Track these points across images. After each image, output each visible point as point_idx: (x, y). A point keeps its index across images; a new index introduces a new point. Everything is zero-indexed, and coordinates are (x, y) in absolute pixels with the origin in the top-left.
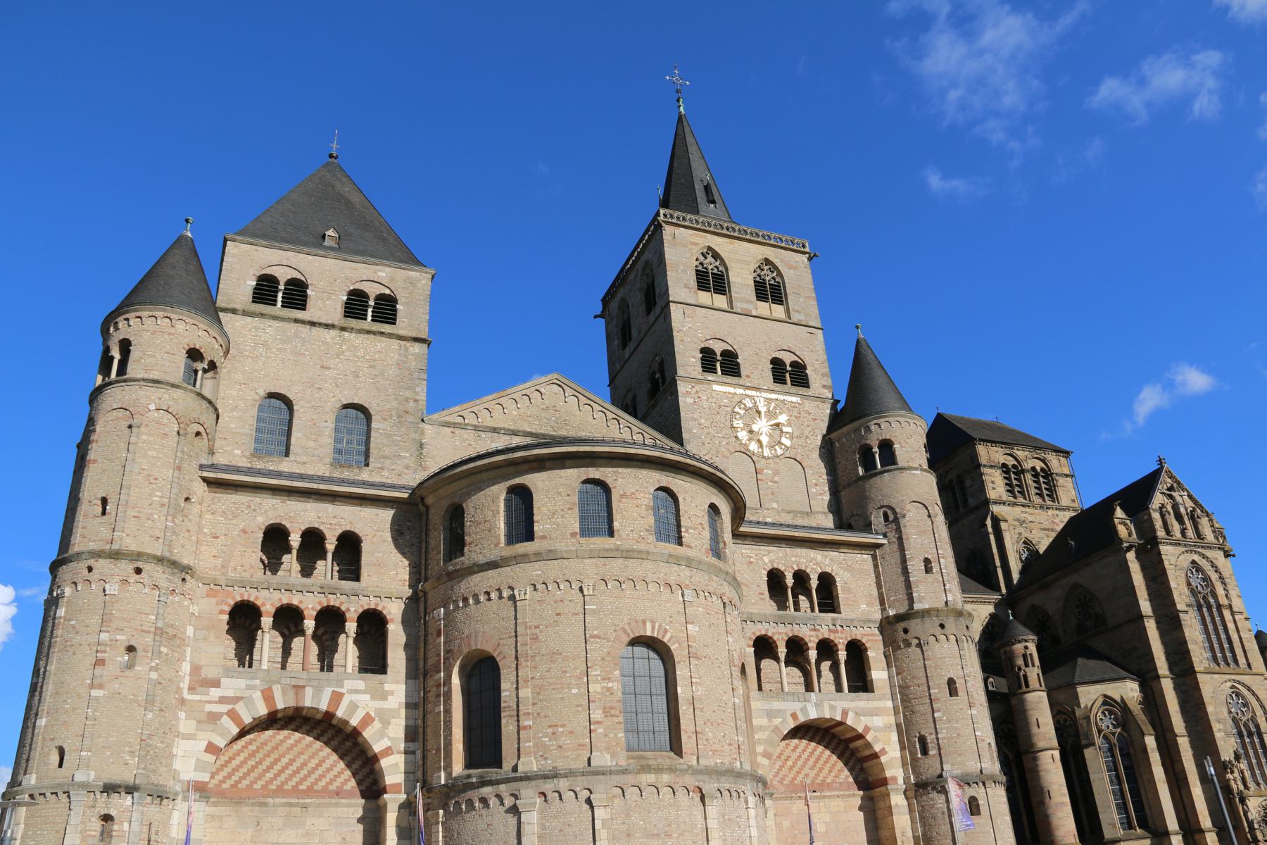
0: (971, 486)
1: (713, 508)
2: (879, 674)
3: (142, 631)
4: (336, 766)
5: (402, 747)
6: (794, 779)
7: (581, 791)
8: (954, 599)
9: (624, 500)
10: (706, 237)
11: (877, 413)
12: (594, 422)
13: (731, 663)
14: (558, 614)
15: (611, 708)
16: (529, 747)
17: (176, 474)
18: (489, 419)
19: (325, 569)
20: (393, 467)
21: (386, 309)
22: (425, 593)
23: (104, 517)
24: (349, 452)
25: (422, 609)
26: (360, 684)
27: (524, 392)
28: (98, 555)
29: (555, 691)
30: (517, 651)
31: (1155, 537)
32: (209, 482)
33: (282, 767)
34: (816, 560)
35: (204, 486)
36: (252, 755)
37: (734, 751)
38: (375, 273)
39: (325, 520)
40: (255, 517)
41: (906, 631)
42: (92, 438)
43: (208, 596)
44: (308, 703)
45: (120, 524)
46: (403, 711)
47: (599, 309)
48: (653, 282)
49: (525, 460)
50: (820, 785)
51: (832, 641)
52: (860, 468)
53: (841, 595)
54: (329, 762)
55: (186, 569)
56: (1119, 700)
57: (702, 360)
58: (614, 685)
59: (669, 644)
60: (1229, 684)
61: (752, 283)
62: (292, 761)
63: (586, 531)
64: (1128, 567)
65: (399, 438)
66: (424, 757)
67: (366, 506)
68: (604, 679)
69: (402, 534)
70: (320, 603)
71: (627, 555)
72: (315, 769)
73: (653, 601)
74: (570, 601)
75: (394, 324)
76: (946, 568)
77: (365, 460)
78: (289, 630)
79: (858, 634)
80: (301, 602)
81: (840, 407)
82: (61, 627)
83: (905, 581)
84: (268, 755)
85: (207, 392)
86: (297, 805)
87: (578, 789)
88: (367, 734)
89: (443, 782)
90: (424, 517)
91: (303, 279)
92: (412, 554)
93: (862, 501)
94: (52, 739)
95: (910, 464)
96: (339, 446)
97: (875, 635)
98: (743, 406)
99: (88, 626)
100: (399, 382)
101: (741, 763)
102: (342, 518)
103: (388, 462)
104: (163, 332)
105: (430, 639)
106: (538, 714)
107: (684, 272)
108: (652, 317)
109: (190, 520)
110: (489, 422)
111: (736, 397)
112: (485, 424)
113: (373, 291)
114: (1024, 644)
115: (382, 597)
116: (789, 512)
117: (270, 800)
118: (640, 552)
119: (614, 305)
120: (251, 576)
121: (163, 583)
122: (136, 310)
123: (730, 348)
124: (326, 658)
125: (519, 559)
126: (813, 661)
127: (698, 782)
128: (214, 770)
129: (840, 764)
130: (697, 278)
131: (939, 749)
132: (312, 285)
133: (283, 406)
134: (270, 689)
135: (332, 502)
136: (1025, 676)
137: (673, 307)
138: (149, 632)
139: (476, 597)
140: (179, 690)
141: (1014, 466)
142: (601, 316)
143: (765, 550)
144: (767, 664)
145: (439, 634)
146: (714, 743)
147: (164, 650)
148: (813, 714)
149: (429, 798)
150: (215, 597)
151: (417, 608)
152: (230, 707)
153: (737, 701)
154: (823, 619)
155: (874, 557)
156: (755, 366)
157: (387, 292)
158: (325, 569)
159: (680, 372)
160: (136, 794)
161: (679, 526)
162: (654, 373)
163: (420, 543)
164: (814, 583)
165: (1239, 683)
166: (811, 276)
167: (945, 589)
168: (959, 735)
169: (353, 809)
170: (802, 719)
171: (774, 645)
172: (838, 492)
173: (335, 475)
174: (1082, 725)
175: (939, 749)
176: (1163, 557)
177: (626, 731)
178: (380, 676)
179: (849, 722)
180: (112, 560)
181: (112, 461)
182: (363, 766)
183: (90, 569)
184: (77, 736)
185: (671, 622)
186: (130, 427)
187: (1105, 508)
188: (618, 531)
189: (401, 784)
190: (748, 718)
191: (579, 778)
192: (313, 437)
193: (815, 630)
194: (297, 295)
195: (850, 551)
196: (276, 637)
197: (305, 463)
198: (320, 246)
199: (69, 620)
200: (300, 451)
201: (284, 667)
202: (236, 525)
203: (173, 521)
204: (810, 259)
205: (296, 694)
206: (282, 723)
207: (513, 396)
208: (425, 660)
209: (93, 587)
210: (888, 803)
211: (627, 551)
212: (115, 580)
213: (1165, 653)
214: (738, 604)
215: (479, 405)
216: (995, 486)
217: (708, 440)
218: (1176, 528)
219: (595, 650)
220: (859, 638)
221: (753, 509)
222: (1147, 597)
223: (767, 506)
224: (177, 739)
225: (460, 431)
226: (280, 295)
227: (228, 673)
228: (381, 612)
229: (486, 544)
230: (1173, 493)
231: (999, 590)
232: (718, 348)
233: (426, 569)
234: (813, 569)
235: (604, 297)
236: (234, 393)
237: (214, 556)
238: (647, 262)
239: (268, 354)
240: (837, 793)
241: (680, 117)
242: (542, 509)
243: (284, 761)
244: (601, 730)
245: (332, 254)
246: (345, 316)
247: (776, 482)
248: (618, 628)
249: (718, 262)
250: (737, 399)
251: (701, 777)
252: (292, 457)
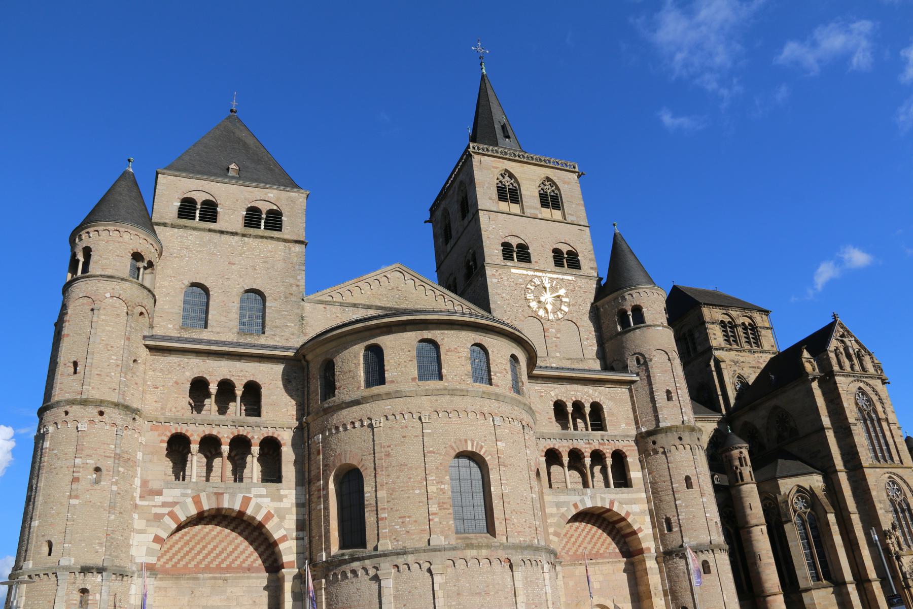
1: (514, 358)
2: (636, 474)
3: (105, 456)
4: (247, 550)
5: (294, 534)
6: (577, 551)
7: (423, 563)
8: (689, 419)
9: (449, 354)
10: (503, 163)
11: (630, 286)
12: (426, 298)
13: (529, 469)
14: (404, 437)
15: (444, 503)
16: (386, 532)
17: (127, 342)
18: (350, 297)
19: (236, 408)
20: (283, 334)
21: (275, 220)
22: (308, 424)
23: (76, 375)
24: (250, 324)
25: (306, 435)
27: (375, 278)
28: (72, 402)
29: (403, 492)
30: (375, 464)
31: (832, 371)
32: (151, 348)
33: (209, 552)
34: (588, 393)
35: (146, 351)
36: (187, 543)
37: (533, 532)
38: (266, 194)
39: (234, 373)
40: (184, 372)
41: (654, 443)
42: (65, 319)
43: (151, 430)
44: (226, 505)
45: (87, 380)
46: (294, 510)
47: (428, 216)
48: (466, 196)
49: (377, 327)
50: (595, 555)
51: (602, 451)
52: (619, 327)
53: (607, 419)
54: (242, 547)
55: (136, 411)
56: (808, 488)
57: (503, 251)
58: (445, 487)
59: (484, 456)
60: (887, 475)
62: (215, 547)
63: (422, 377)
64: (813, 393)
65: (286, 313)
66: (310, 542)
67: (264, 362)
68: (438, 483)
69: (290, 382)
70: (232, 433)
71: (453, 393)
72: (232, 552)
73: (472, 425)
74: (413, 427)
75: (281, 231)
76: (682, 397)
77: (262, 329)
78: (211, 453)
79: (620, 445)
80: (219, 433)
81: (603, 282)
82: (47, 455)
83: (653, 407)
84: (198, 543)
85: (147, 284)
86: (220, 578)
87: (421, 562)
88: (269, 526)
89: (324, 560)
90: (306, 370)
91: (214, 200)
92: (298, 397)
93: (621, 350)
94: (43, 536)
95: (655, 323)
96: (243, 320)
97: (632, 446)
98: (533, 284)
99: (66, 454)
100: (285, 273)
101: (538, 540)
102: (246, 372)
103: (278, 330)
104: (114, 241)
105: (312, 457)
106: (391, 509)
107: (489, 188)
108: (466, 221)
109: (137, 376)
110: (351, 300)
111: (528, 277)
112: (348, 301)
113: (264, 207)
114: (739, 450)
115: (277, 428)
116: (568, 359)
117: (200, 575)
118: (462, 390)
119: (439, 213)
120: (183, 415)
121: (119, 422)
122: (94, 226)
123: (523, 242)
124: (238, 473)
125: (375, 398)
126: (588, 466)
127: (507, 554)
128: (160, 555)
129: (609, 540)
130: (498, 192)
131: (680, 527)
132: (220, 204)
133: (202, 292)
134: (198, 496)
135: (239, 360)
136: (741, 473)
137: (481, 213)
138: (110, 457)
139: (344, 426)
140: (133, 498)
141: (729, 322)
142: (430, 221)
143: (552, 387)
144: (555, 469)
145: (319, 454)
146: (518, 527)
147: (121, 469)
148: (589, 504)
149: (314, 571)
150: (157, 430)
151: (302, 435)
152: (170, 509)
153: (534, 496)
154: (594, 435)
155: (630, 390)
156: (541, 254)
157: (275, 208)
158: (236, 408)
159: (488, 260)
160: (104, 574)
161: (489, 371)
162: (469, 262)
163: (303, 388)
164: (588, 410)
165: (894, 474)
166: (580, 189)
167: (682, 412)
168: (694, 516)
169: (260, 580)
170: (581, 508)
171: (560, 455)
172: (603, 344)
173: (241, 341)
174: (782, 507)
175: (680, 527)
176: (838, 385)
177: (455, 519)
178: (277, 484)
179: (615, 509)
180: (82, 406)
181: (80, 334)
182: (266, 550)
183: (67, 413)
184: (61, 533)
185: (485, 440)
186: (92, 310)
187: (795, 351)
188: (446, 375)
189: (294, 562)
190: (543, 508)
191: (422, 554)
192: (225, 314)
193: (589, 443)
194: (210, 212)
195: (613, 386)
196: (201, 458)
197: (218, 333)
198: (226, 176)
199: (53, 450)
200: (215, 324)
201: (208, 480)
202: (170, 378)
203: (125, 377)
204: (579, 176)
205: (217, 499)
206: (208, 520)
207: (367, 280)
208: (309, 472)
209: (69, 425)
210: (644, 567)
211: (453, 390)
212: (85, 421)
213: (841, 454)
214: (533, 426)
215: (343, 288)
216: (716, 336)
217: (509, 309)
218: (847, 364)
219: (431, 462)
220: (620, 448)
221: (542, 357)
222: (827, 414)
223: (552, 355)
224: (132, 533)
225: (330, 306)
226: (198, 212)
227: (168, 485)
228: (276, 439)
229: (350, 387)
230: (844, 339)
231: (720, 412)
232: (514, 242)
233: (308, 407)
234: (586, 399)
235: (431, 208)
236: (166, 283)
237: (156, 401)
238: (461, 182)
239: (190, 255)
240: (607, 560)
241: (483, 76)
242: (391, 361)
243: (210, 547)
244: (437, 520)
245: (234, 182)
246: (245, 226)
247: (558, 338)
248: (447, 446)
249: (513, 180)
250: (529, 279)
251: (510, 551)
252: (209, 329)
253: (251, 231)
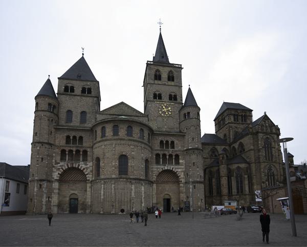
26: (83, 163)
61: (167, 77)
79: (178, 153)
88: (84, 171)
113: (87, 87)
148: (166, 168)
170: (164, 169)
232: (157, 93)
253: (83, 94)
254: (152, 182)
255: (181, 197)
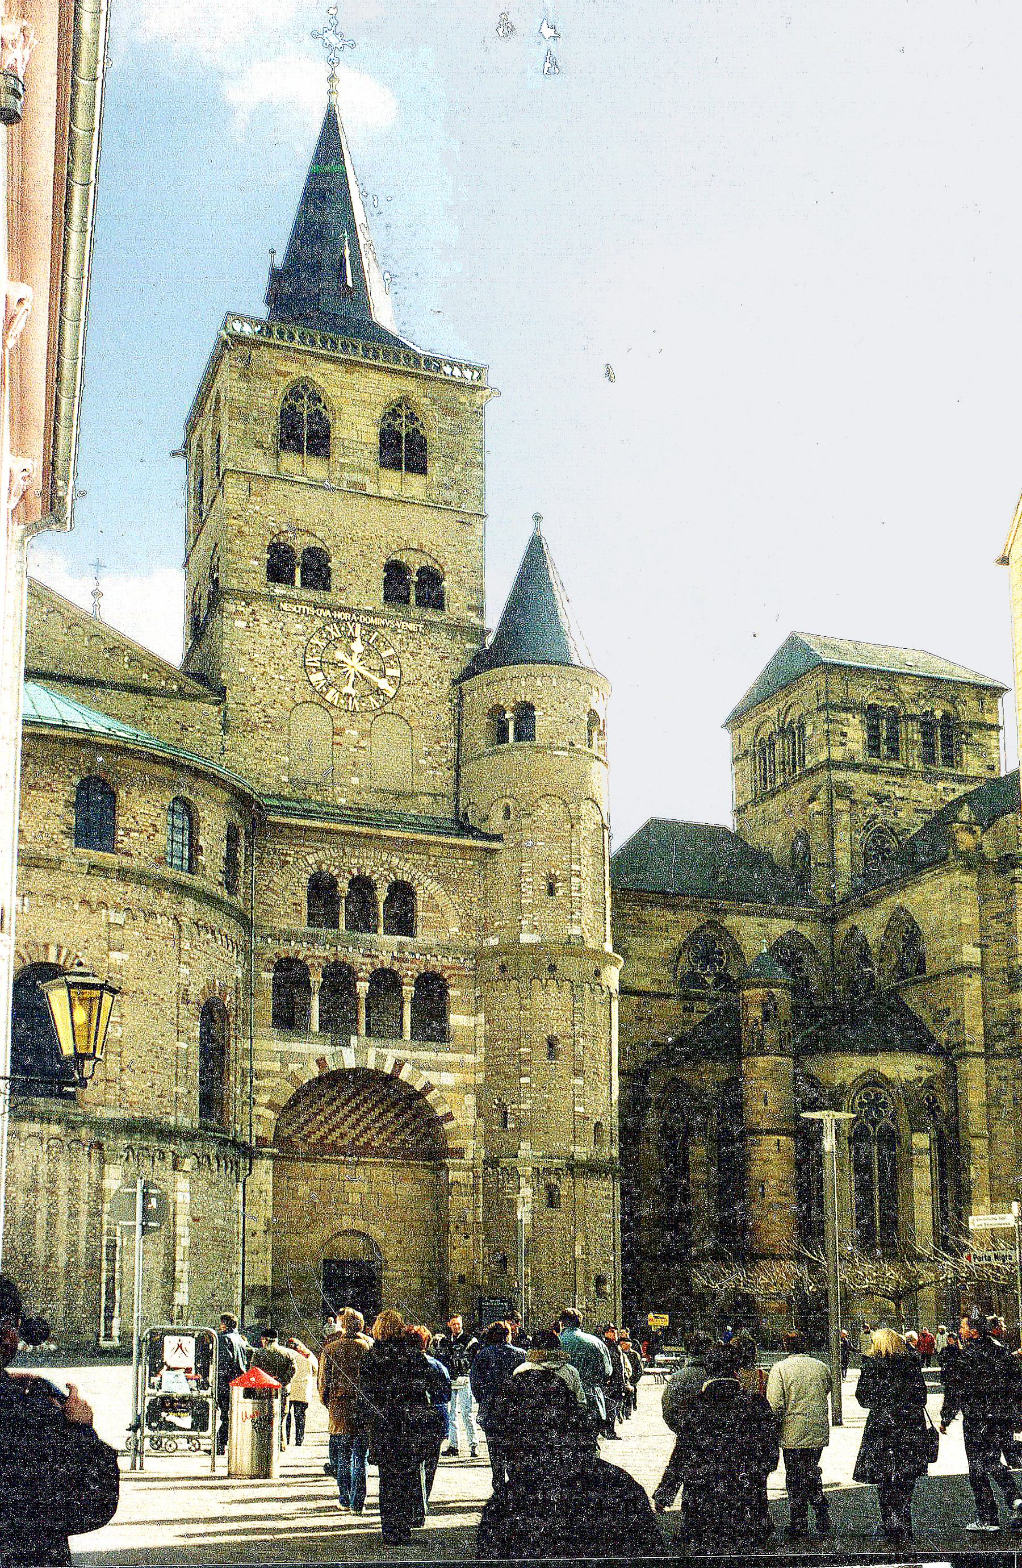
0: (812, 736)
79: (437, 963)
126: (363, 996)
146: (134, 1094)
220: (439, 970)
250: (318, 623)
254: (248, 1152)
255: (455, 1254)
